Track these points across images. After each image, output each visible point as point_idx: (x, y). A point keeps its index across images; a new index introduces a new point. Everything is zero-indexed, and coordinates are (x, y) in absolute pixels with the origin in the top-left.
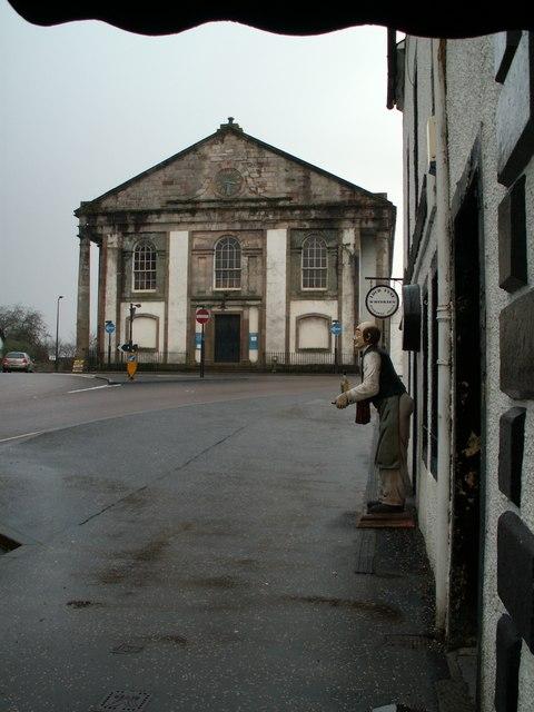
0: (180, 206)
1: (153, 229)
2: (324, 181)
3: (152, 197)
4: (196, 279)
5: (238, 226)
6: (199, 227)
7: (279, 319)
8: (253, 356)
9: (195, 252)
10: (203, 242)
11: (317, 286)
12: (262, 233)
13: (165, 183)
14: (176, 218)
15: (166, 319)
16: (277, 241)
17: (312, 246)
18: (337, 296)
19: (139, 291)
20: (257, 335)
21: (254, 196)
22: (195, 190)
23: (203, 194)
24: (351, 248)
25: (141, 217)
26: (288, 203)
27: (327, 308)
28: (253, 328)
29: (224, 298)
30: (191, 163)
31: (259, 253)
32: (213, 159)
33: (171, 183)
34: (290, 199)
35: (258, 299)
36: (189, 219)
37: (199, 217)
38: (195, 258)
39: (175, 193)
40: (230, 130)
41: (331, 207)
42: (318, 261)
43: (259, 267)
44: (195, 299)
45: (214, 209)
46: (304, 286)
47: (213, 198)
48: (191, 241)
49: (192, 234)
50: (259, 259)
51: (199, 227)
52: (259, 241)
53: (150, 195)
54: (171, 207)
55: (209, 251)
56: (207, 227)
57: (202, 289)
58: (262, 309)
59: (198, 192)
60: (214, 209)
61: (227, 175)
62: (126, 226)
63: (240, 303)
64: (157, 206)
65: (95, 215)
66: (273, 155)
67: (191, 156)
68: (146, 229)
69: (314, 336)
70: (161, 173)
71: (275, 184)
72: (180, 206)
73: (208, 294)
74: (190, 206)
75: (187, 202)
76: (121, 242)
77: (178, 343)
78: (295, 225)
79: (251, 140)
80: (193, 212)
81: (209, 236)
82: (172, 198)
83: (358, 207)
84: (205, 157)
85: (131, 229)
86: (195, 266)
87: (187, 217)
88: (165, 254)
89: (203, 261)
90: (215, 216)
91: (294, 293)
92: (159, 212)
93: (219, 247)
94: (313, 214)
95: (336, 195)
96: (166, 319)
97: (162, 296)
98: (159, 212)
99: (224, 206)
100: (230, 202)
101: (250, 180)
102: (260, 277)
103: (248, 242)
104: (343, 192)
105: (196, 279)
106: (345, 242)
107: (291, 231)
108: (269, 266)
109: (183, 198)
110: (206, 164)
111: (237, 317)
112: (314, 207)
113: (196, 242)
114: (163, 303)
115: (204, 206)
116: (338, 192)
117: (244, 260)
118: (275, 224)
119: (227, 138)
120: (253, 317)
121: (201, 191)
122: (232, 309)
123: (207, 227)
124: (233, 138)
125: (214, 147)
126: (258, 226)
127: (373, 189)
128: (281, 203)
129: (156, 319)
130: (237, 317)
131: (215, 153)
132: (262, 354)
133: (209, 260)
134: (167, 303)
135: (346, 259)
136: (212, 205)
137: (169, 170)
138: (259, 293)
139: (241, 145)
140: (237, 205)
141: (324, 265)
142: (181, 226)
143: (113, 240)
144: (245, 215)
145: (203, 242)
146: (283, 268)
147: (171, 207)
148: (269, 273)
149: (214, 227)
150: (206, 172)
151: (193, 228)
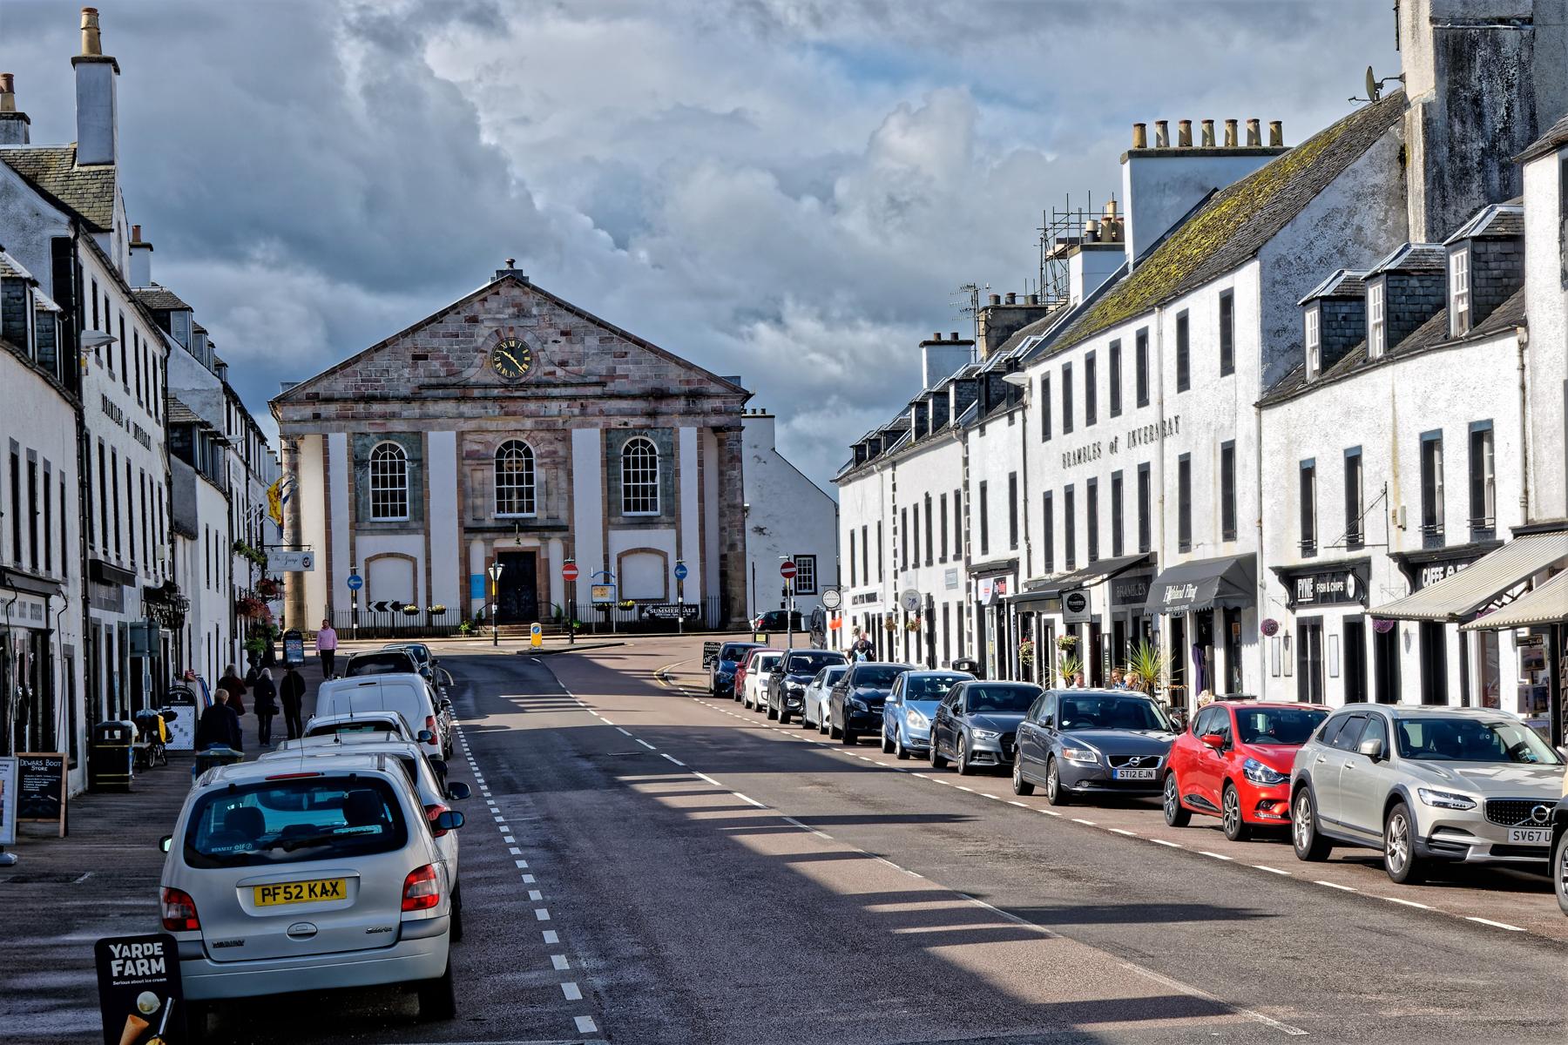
4: (470, 501)
9: (464, 457)
11: (645, 509)
15: (428, 560)
16: (587, 444)
19: (381, 519)
23: (473, 374)
35: (563, 529)
41: (660, 395)
42: (645, 474)
43: (564, 485)
44: (470, 530)
46: (627, 509)
48: (459, 445)
51: (471, 425)
59: (465, 375)
66: (576, 319)
69: (644, 580)
70: (408, 342)
73: (489, 522)
77: (448, 596)
78: (615, 422)
82: (426, 381)
88: (421, 463)
90: (493, 409)
93: (500, 453)
96: (428, 560)
107: (607, 431)
117: (539, 474)
120: (554, 549)
122: (529, 542)
124: (516, 292)
129: (413, 560)
130: (529, 557)
134: (427, 535)
138: (563, 521)
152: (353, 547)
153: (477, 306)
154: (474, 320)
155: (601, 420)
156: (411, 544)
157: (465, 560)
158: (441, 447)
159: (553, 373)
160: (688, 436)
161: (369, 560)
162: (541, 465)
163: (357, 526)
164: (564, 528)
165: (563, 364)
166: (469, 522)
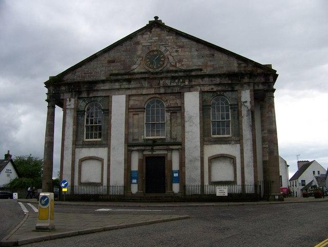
0: (119, 77)
1: (100, 94)
2: (225, 57)
3: (100, 71)
4: (131, 130)
5: (162, 91)
6: (134, 92)
7: (196, 159)
8: (176, 188)
9: (130, 109)
10: (137, 102)
12: (180, 95)
13: (110, 62)
14: (117, 85)
15: (109, 160)
16: (192, 101)
17: (218, 104)
18: (238, 138)
20: (178, 172)
21: (174, 69)
22: (130, 66)
23: (137, 68)
24: (248, 104)
25: (92, 85)
26: (199, 73)
27: (231, 150)
28: (176, 166)
29: (154, 143)
30: (128, 48)
31: (178, 110)
32: (143, 44)
33: (113, 62)
34: (201, 70)
35: (178, 145)
36: (126, 86)
37: (133, 85)
38: (131, 114)
39: (116, 68)
40: (156, 24)
41: (231, 75)
43: (179, 121)
44: (130, 146)
45: (145, 79)
47: (143, 71)
48: (128, 101)
49: (129, 97)
50: (178, 115)
51: (134, 92)
52: (178, 101)
53: (98, 70)
54: (113, 78)
55: (142, 109)
56: (140, 92)
57: (136, 137)
58: (182, 151)
60: (145, 79)
61: (154, 56)
62: (80, 92)
63: (165, 147)
64: (103, 78)
65: (59, 86)
66: (187, 40)
67: (128, 43)
68: (95, 94)
69: (222, 172)
70: (106, 55)
71: (192, 60)
72: (119, 77)
73: (141, 141)
74: (127, 77)
75: (125, 74)
76: (77, 105)
77: (118, 178)
78: (206, 89)
79: (171, 30)
80: (129, 81)
81: (141, 98)
83: (251, 75)
84: (138, 43)
85: (84, 95)
86: (131, 120)
87: (125, 85)
88: (107, 112)
89: (136, 117)
90: (146, 84)
91: (206, 139)
92: (103, 82)
93: (148, 106)
94: (218, 80)
95: (235, 66)
96: (109, 160)
97: (106, 144)
98: (103, 82)
99: (150, 77)
100: (157, 73)
101: (171, 58)
102: (180, 128)
103: (172, 101)
104: (239, 64)
105: (131, 130)
106: (243, 100)
107: (202, 93)
108: (186, 119)
109: (123, 72)
110: (140, 47)
111: (162, 158)
112: (220, 76)
113: (132, 103)
114: (106, 149)
115: (137, 76)
116: (236, 65)
118: (190, 88)
119: (153, 30)
121: (134, 67)
122: (159, 152)
123: (140, 92)
124: (158, 30)
125: (144, 36)
126: (176, 90)
127: (263, 63)
128: (193, 73)
129: (101, 160)
130: (162, 158)
131: (145, 40)
132: (183, 187)
133: (141, 115)
135: (244, 112)
136: (143, 76)
137: (112, 54)
138: (179, 140)
139: (164, 34)
140: (162, 75)
141: (228, 118)
142: (121, 92)
143: (71, 103)
144: (168, 82)
145: (137, 102)
146: (197, 120)
147: (113, 78)
148: (187, 125)
149: (144, 92)
150: (139, 53)
151: (129, 92)
152: (74, 154)
153: (139, 37)
154: (138, 43)
155: (199, 88)
156: (101, 152)
157: (128, 161)
158: (119, 103)
159: (175, 66)
160: (246, 96)
161: (82, 161)
162: (168, 111)
163: (77, 144)
164: (180, 144)
165: (180, 61)
166: (130, 141)
